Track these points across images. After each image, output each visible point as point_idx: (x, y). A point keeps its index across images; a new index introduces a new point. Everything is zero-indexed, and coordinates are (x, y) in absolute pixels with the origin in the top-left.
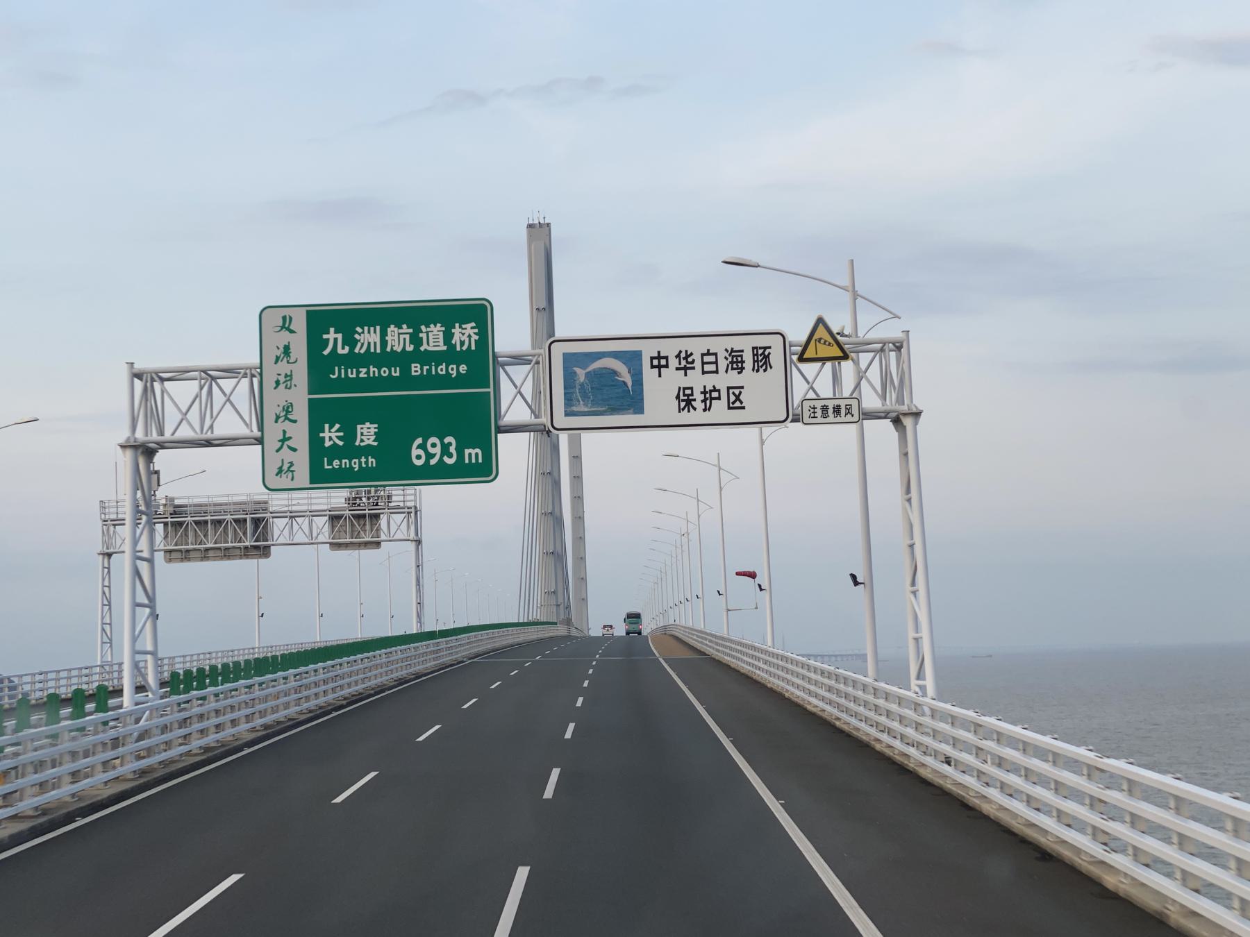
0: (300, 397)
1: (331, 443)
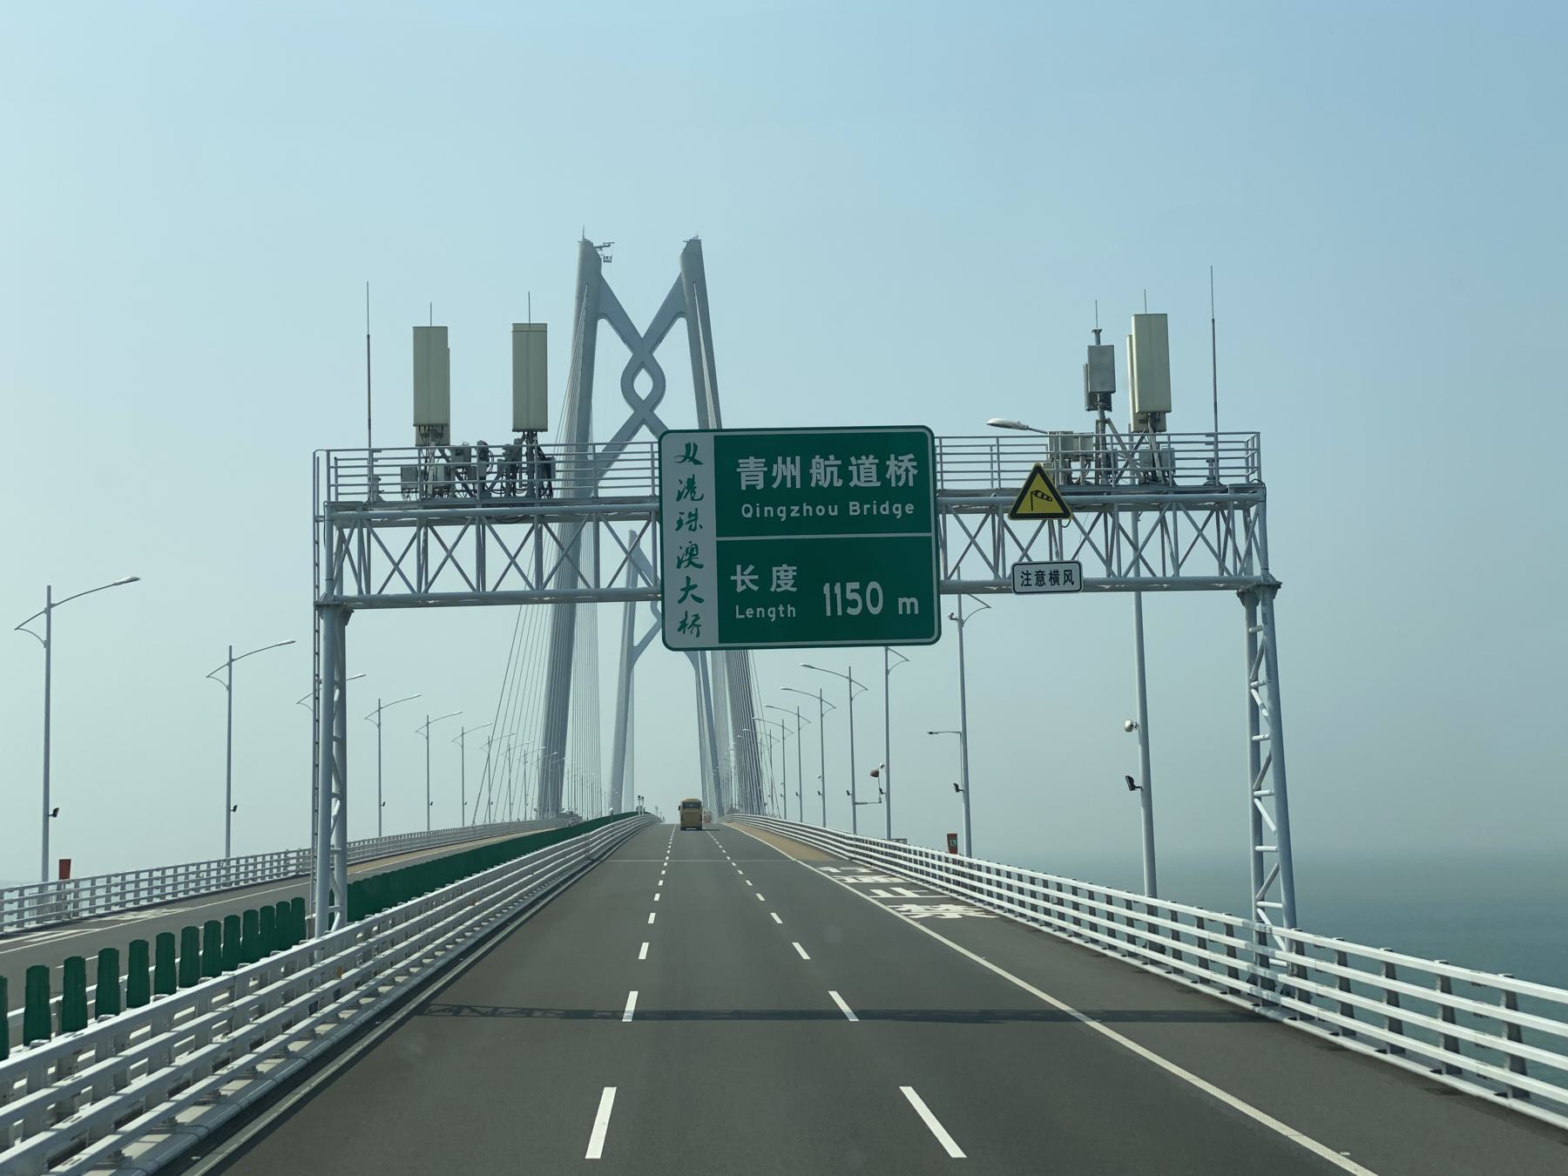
0: (707, 539)
1: (744, 587)
